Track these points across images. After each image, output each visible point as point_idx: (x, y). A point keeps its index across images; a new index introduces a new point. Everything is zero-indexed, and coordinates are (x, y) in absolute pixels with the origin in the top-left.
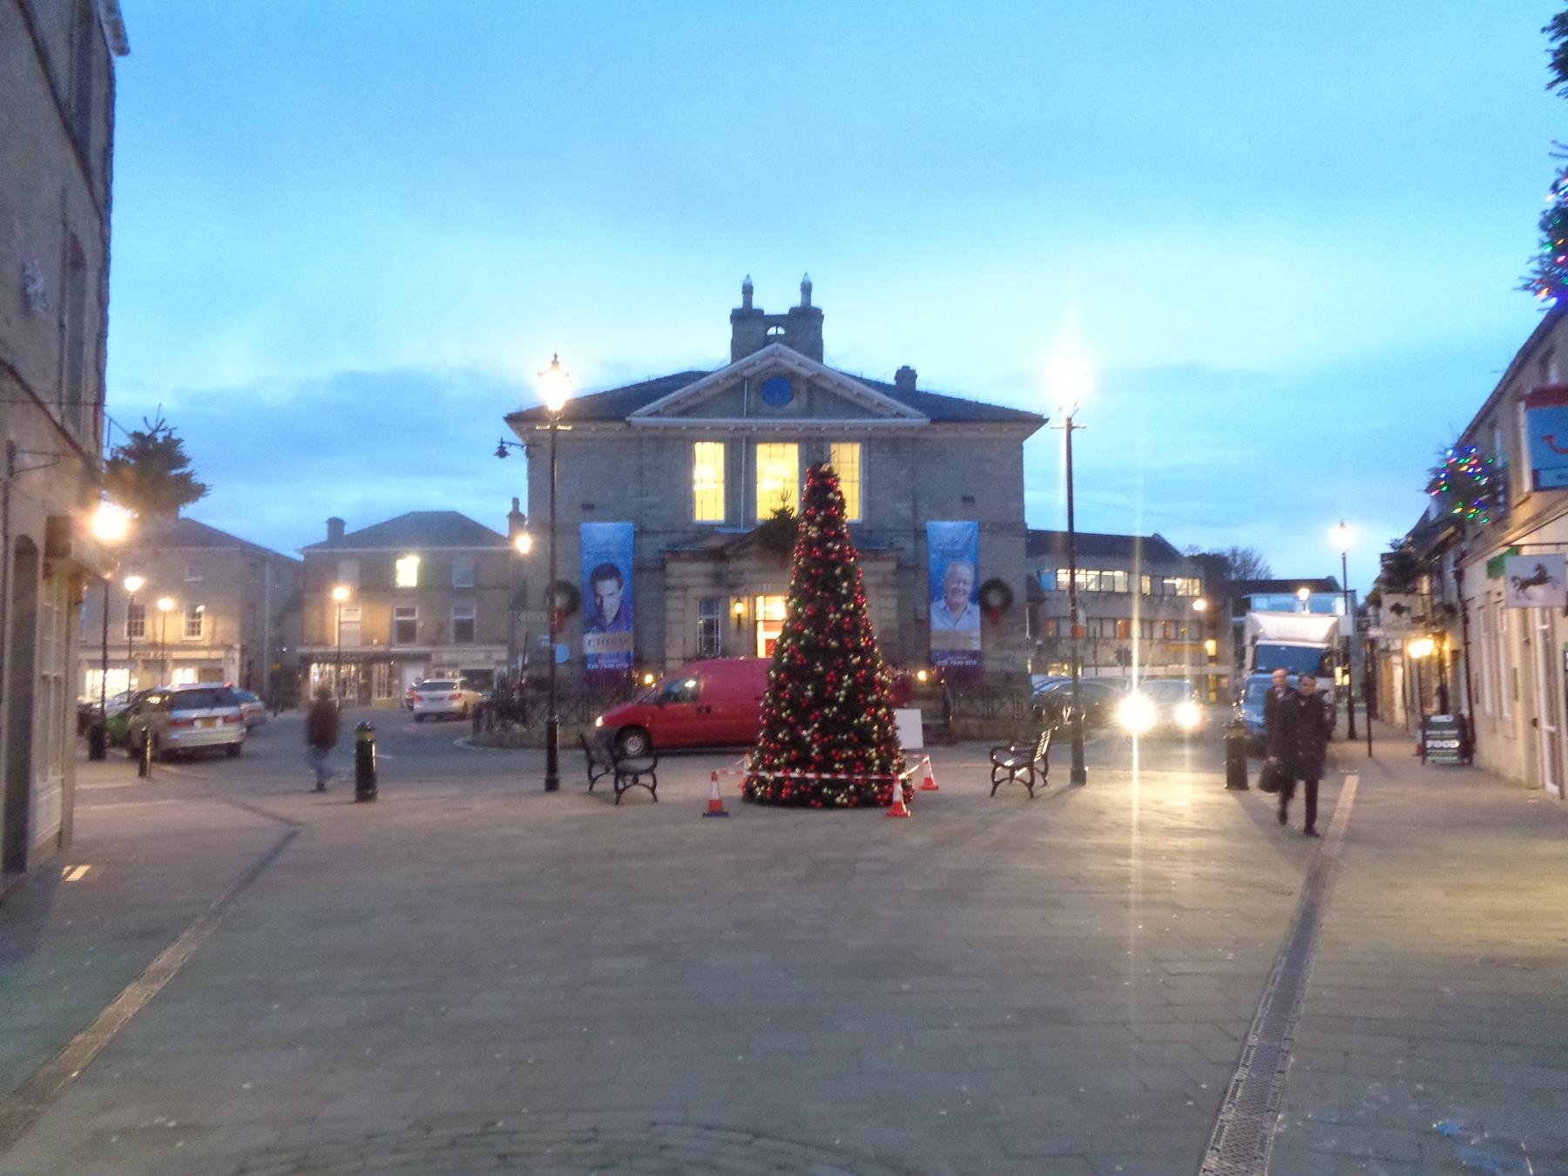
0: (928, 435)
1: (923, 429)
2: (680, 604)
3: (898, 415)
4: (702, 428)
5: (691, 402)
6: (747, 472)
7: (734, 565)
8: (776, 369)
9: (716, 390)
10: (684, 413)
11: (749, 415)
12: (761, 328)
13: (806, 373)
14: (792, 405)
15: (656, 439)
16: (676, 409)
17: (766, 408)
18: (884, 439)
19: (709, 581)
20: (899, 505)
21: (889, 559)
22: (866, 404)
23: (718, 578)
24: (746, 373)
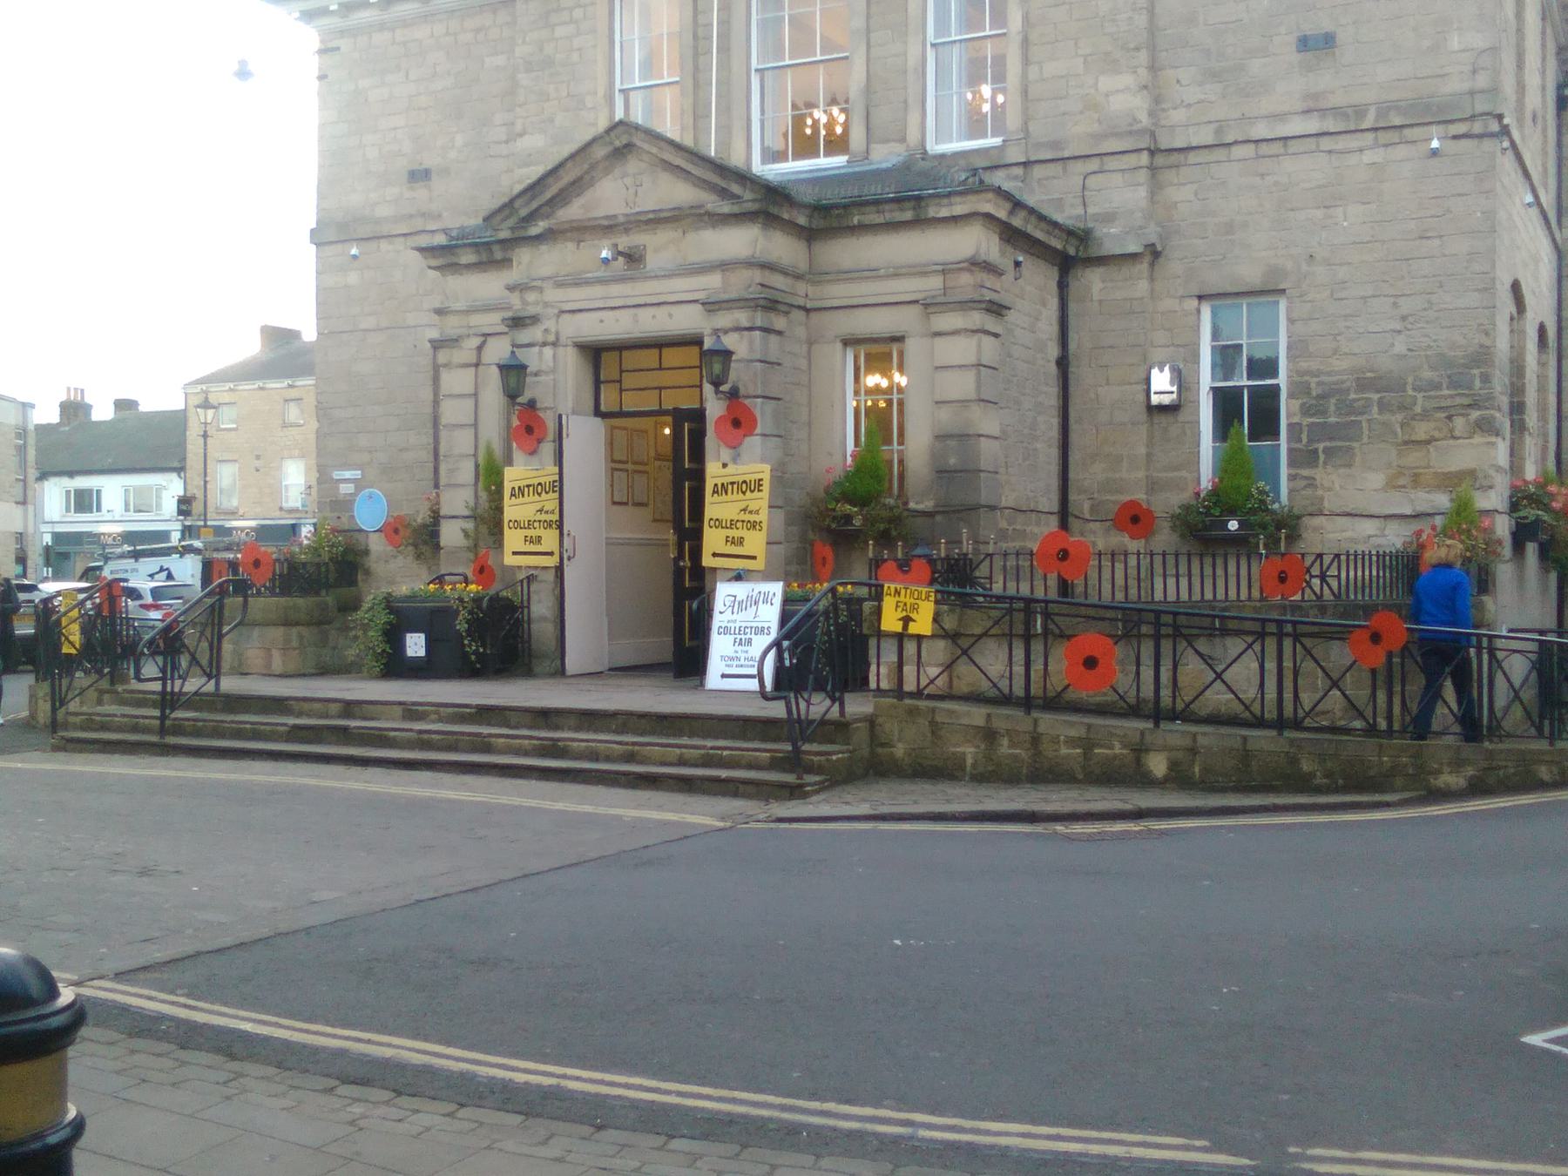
6: (724, 49)
20: (1106, 83)
21: (954, 220)
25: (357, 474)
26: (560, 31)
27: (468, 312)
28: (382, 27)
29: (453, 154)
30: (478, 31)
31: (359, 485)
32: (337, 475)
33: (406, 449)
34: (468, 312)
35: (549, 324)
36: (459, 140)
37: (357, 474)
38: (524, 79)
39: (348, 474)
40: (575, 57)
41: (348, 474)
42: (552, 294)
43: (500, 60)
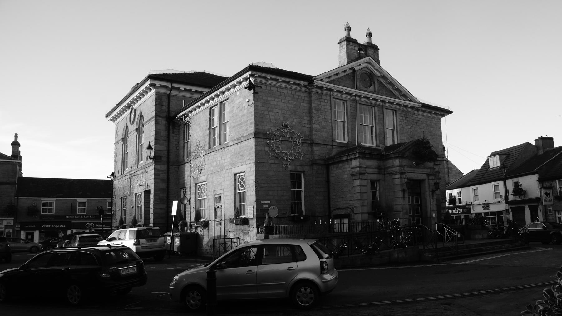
0: (415, 112)
1: (418, 110)
2: (364, 183)
3: (410, 101)
4: (341, 92)
5: (334, 78)
7: (390, 163)
8: (366, 69)
9: (344, 74)
10: (329, 82)
11: (357, 89)
12: (357, 49)
13: (379, 74)
14: (372, 88)
15: (318, 93)
16: (329, 80)
17: (364, 89)
18: (403, 111)
19: (376, 171)
22: (397, 93)
23: (381, 170)
24: (356, 68)
25: (269, 202)
26: (322, 104)
27: (365, 168)
28: (274, 86)
29: (294, 123)
30: (299, 96)
31: (270, 205)
32: (262, 202)
33: (283, 196)
34: (365, 168)
35: (407, 174)
36: (295, 121)
37: (269, 202)
38: (314, 111)
39: (266, 202)
40: (326, 110)
41: (266, 202)
42: (406, 168)
43: (305, 105)
